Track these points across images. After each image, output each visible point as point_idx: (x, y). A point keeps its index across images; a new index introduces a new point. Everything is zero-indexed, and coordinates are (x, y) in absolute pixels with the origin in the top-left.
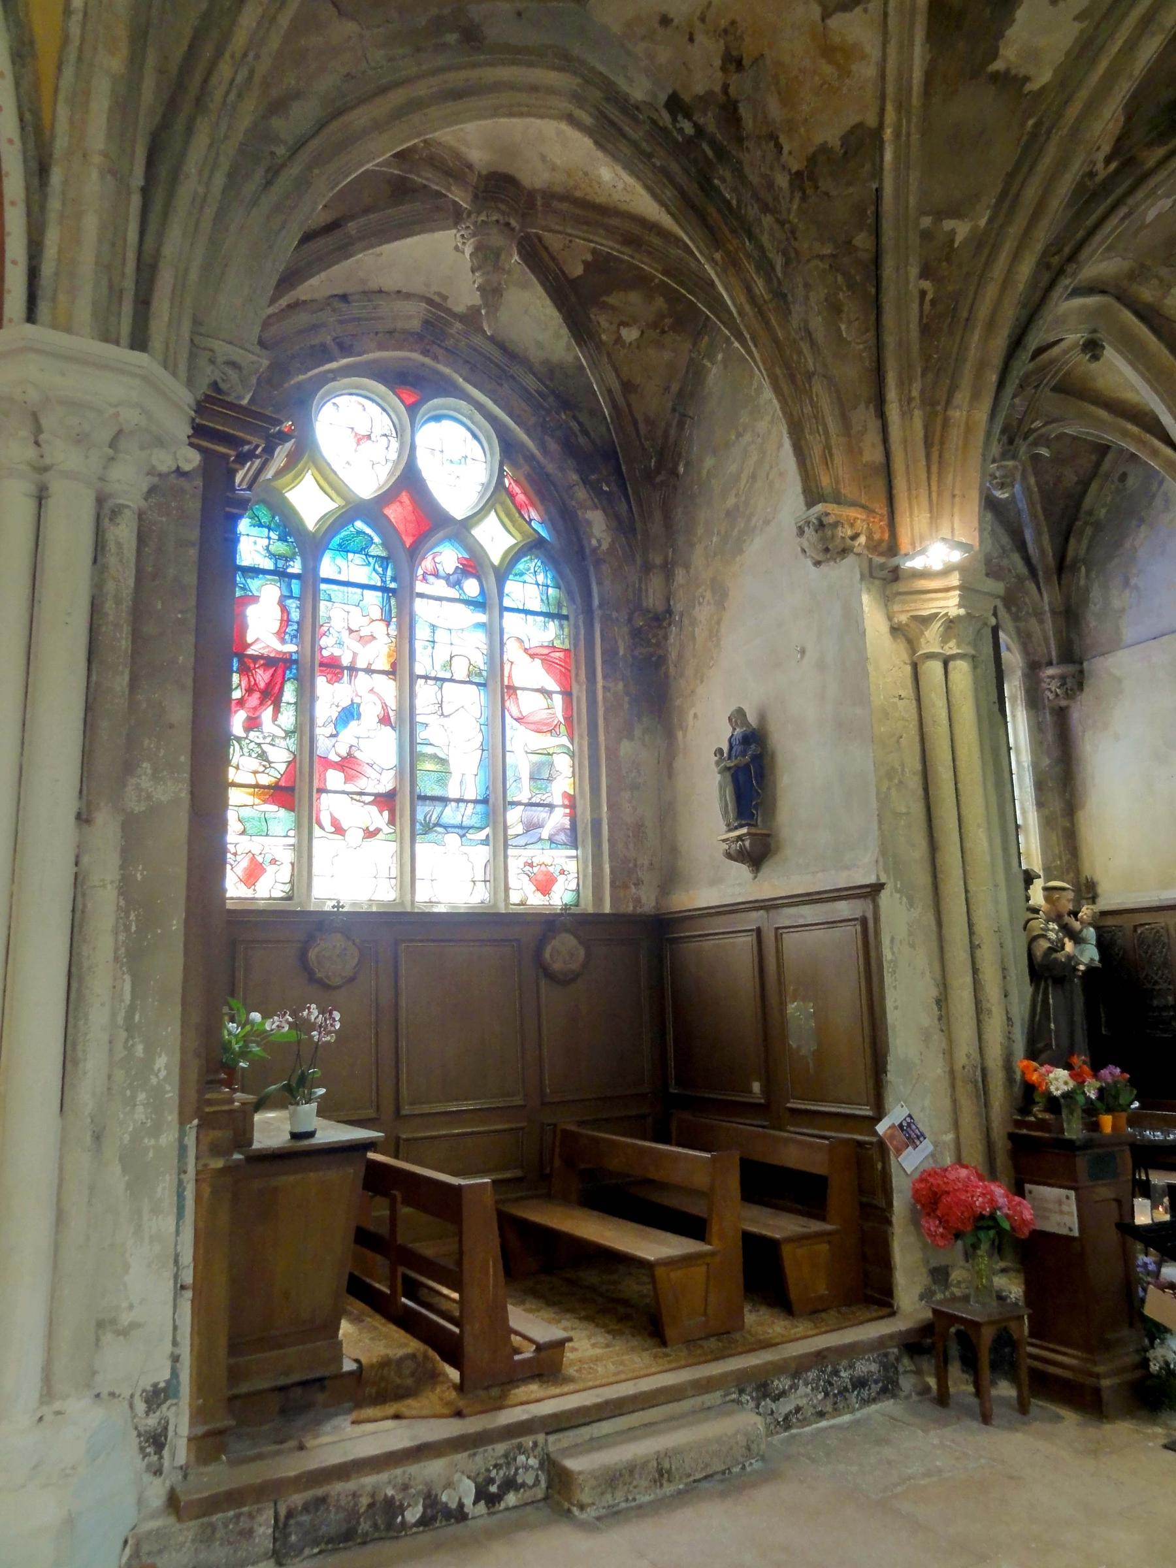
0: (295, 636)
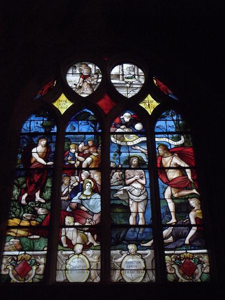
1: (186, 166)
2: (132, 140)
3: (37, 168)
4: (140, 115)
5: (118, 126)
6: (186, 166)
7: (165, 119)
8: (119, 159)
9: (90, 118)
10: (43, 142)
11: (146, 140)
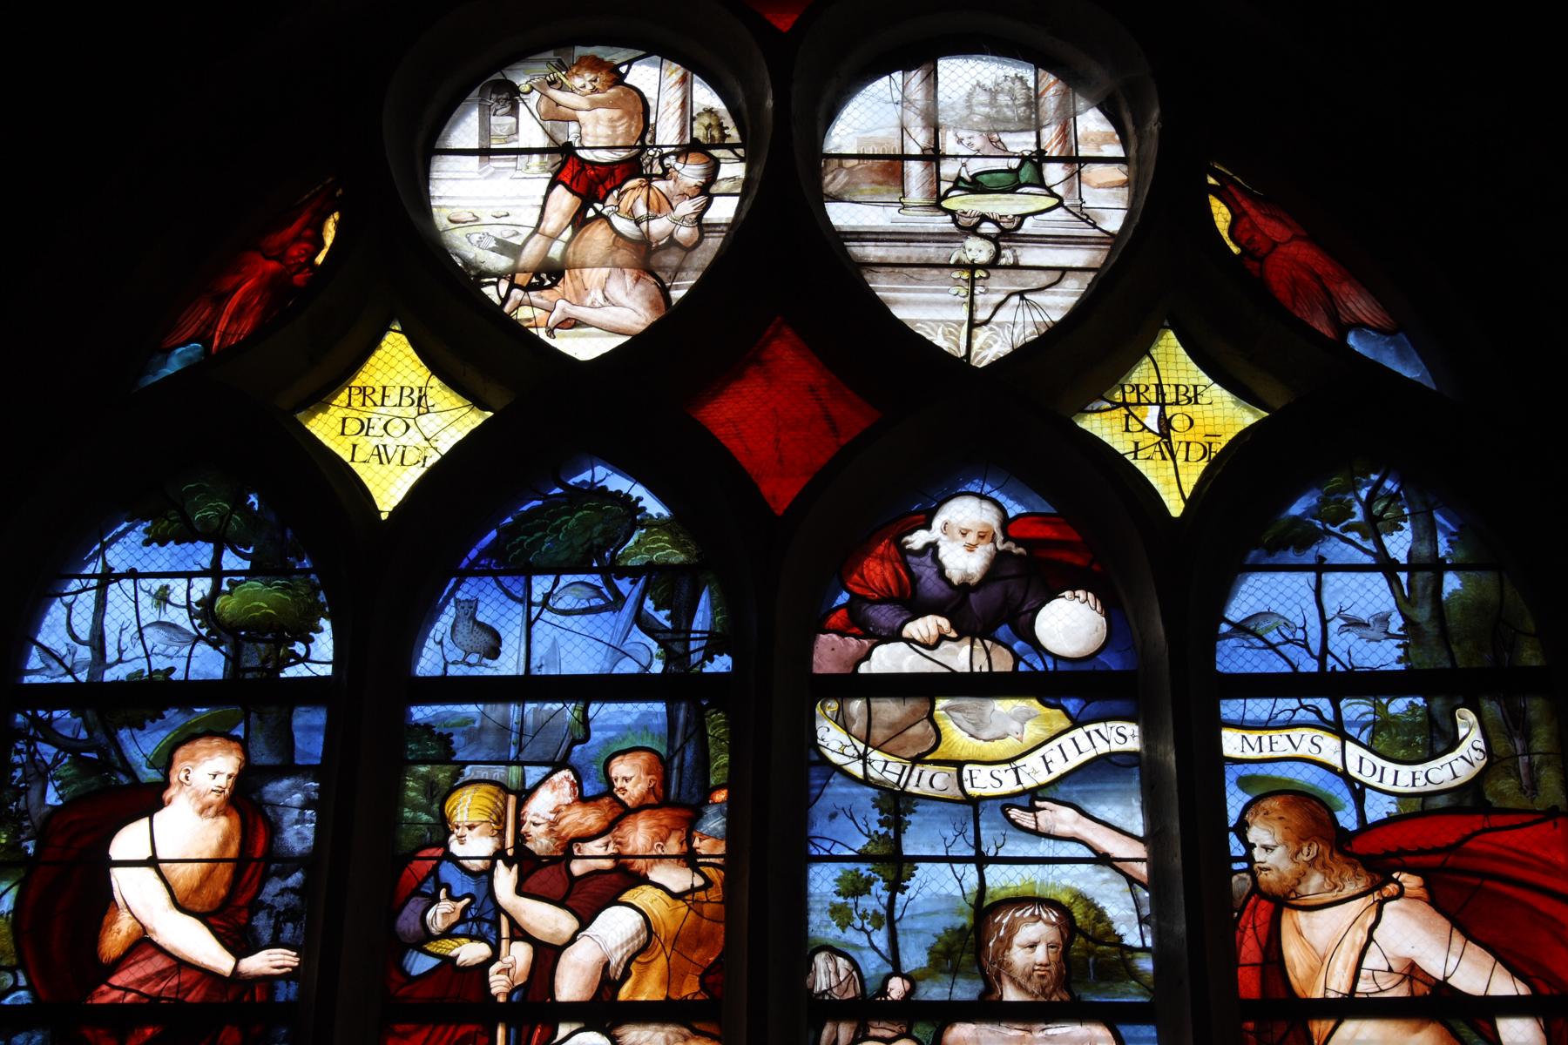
0: (290, 914)
1: (1505, 985)
2: (1011, 744)
3: (148, 1009)
4: (1088, 521)
5: (883, 615)
6: (1505, 985)
7: (1309, 557)
8: (888, 919)
9: (635, 549)
10: (210, 769)
11: (1134, 744)
